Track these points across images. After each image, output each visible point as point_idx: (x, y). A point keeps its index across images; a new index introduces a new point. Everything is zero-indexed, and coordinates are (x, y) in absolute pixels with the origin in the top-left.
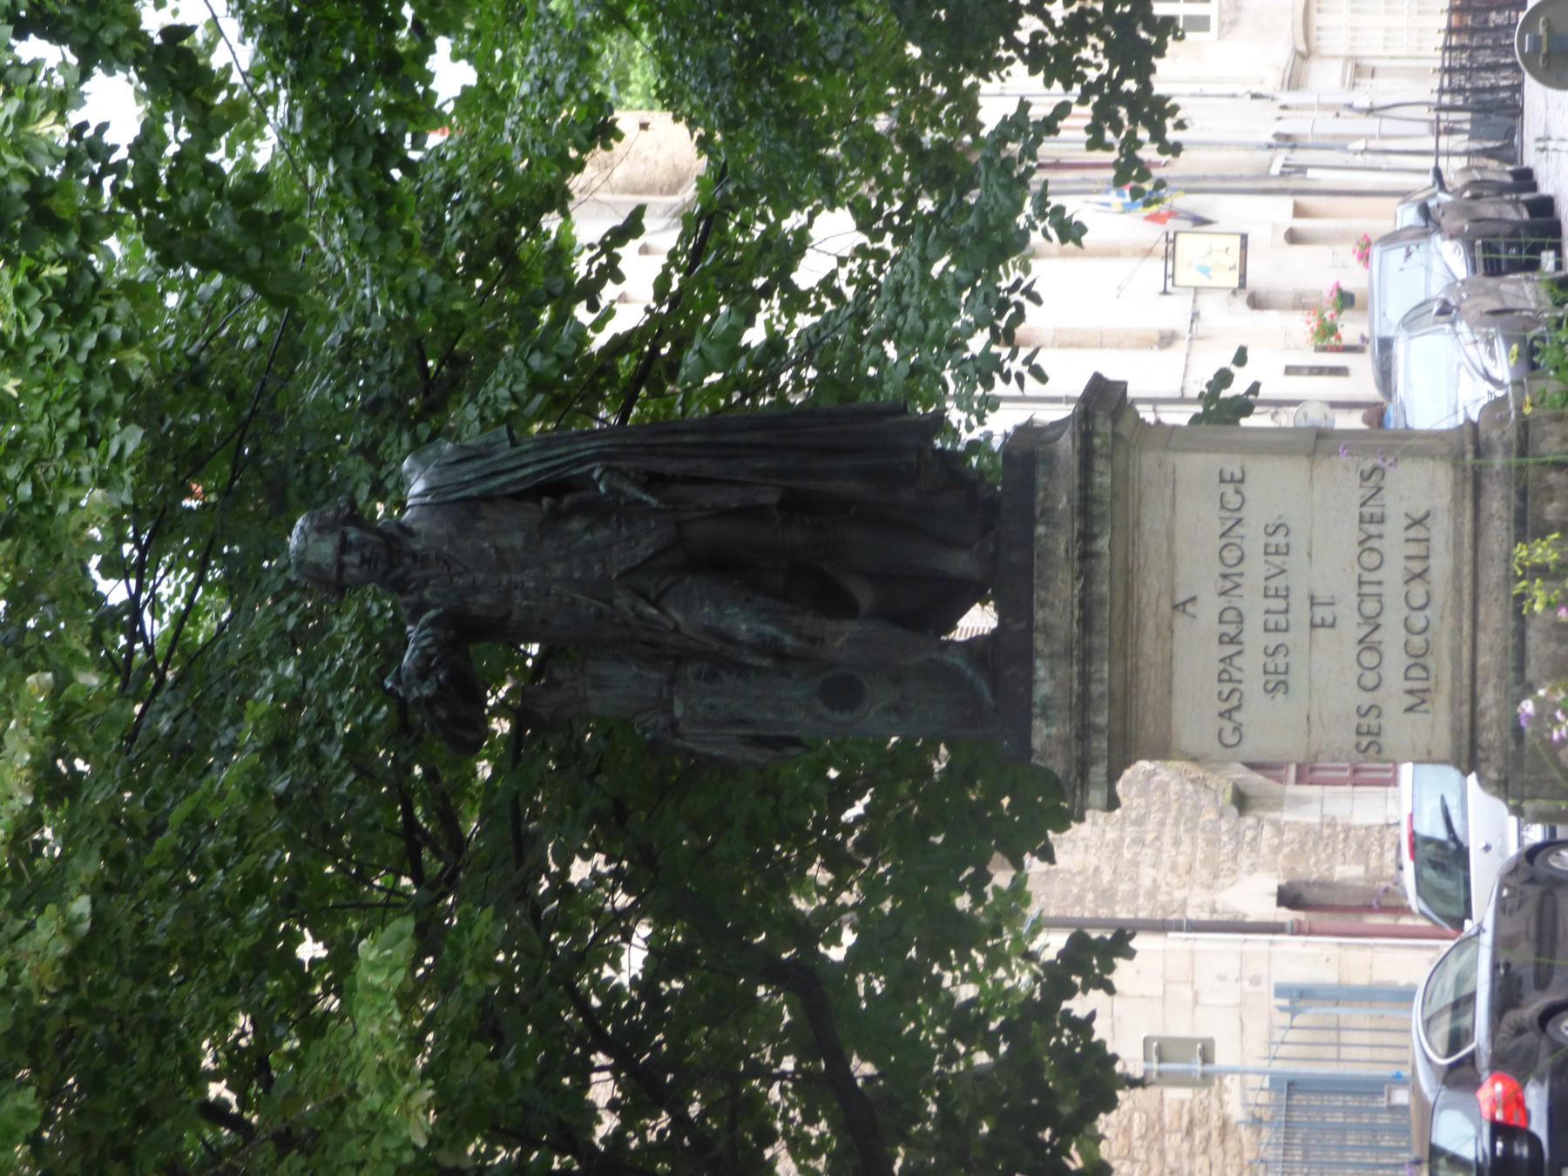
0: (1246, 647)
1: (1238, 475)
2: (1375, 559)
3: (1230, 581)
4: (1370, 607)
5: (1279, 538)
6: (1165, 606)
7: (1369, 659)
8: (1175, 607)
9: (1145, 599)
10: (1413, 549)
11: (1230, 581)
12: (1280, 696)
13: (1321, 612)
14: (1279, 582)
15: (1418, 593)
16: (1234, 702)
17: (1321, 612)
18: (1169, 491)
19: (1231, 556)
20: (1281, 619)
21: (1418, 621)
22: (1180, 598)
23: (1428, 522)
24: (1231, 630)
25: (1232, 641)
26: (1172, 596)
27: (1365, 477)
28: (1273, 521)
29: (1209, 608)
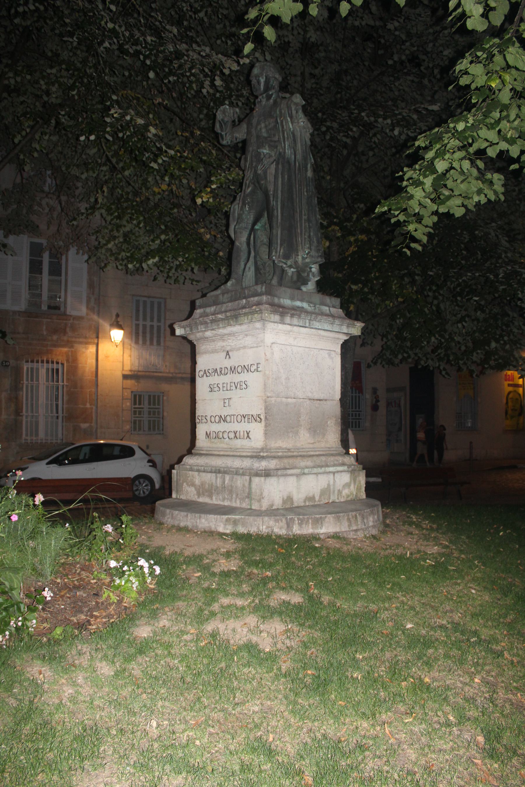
0: (219, 377)
1: (259, 369)
2: (239, 421)
3: (233, 370)
4: (228, 419)
5: (244, 386)
6: (228, 348)
7: (217, 419)
8: (228, 352)
9: (230, 341)
10: (242, 434)
11: (233, 370)
12: (209, 389)
13: (227, 401)
14: (234, 388)
15: (232, 435)
16: (208, 374)
17: (227, 401)
18: (255, 345)
19: (240, 370)
20: (225, 389)
21: (226, 436)
22: (230, 353)
23: (248, 439)
24: (223, 372)
25: (221, 372)
26: (231, 351)
27: (259, 415)
28: (248, 384)
29: (228, 363)
